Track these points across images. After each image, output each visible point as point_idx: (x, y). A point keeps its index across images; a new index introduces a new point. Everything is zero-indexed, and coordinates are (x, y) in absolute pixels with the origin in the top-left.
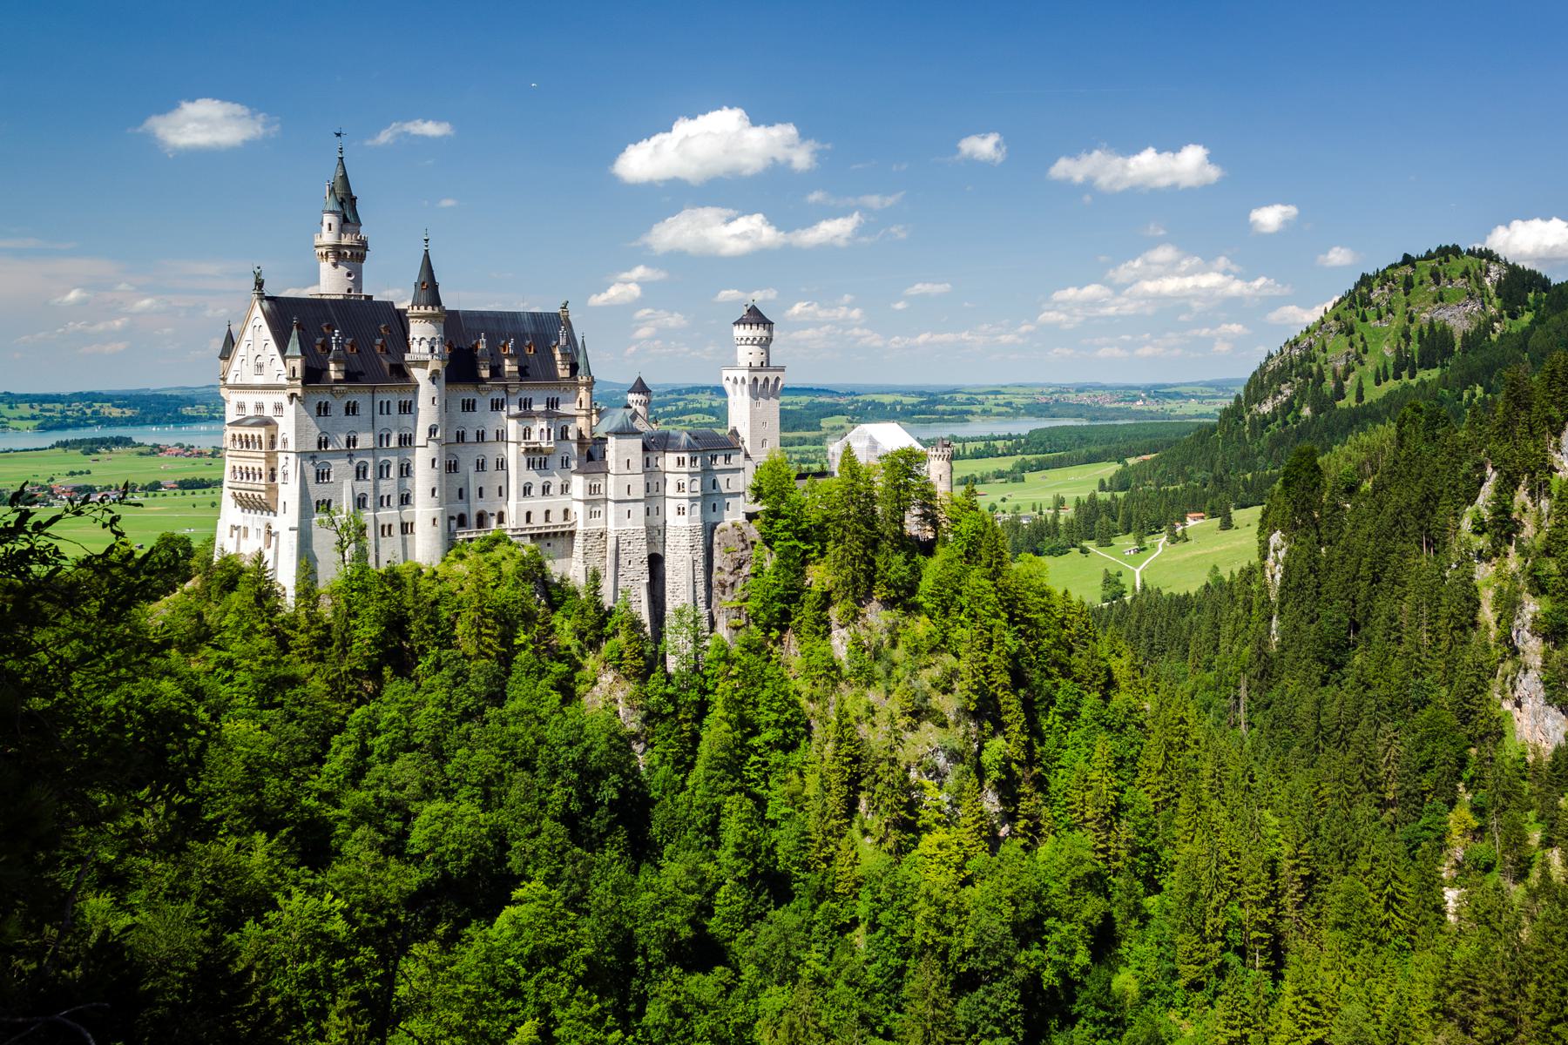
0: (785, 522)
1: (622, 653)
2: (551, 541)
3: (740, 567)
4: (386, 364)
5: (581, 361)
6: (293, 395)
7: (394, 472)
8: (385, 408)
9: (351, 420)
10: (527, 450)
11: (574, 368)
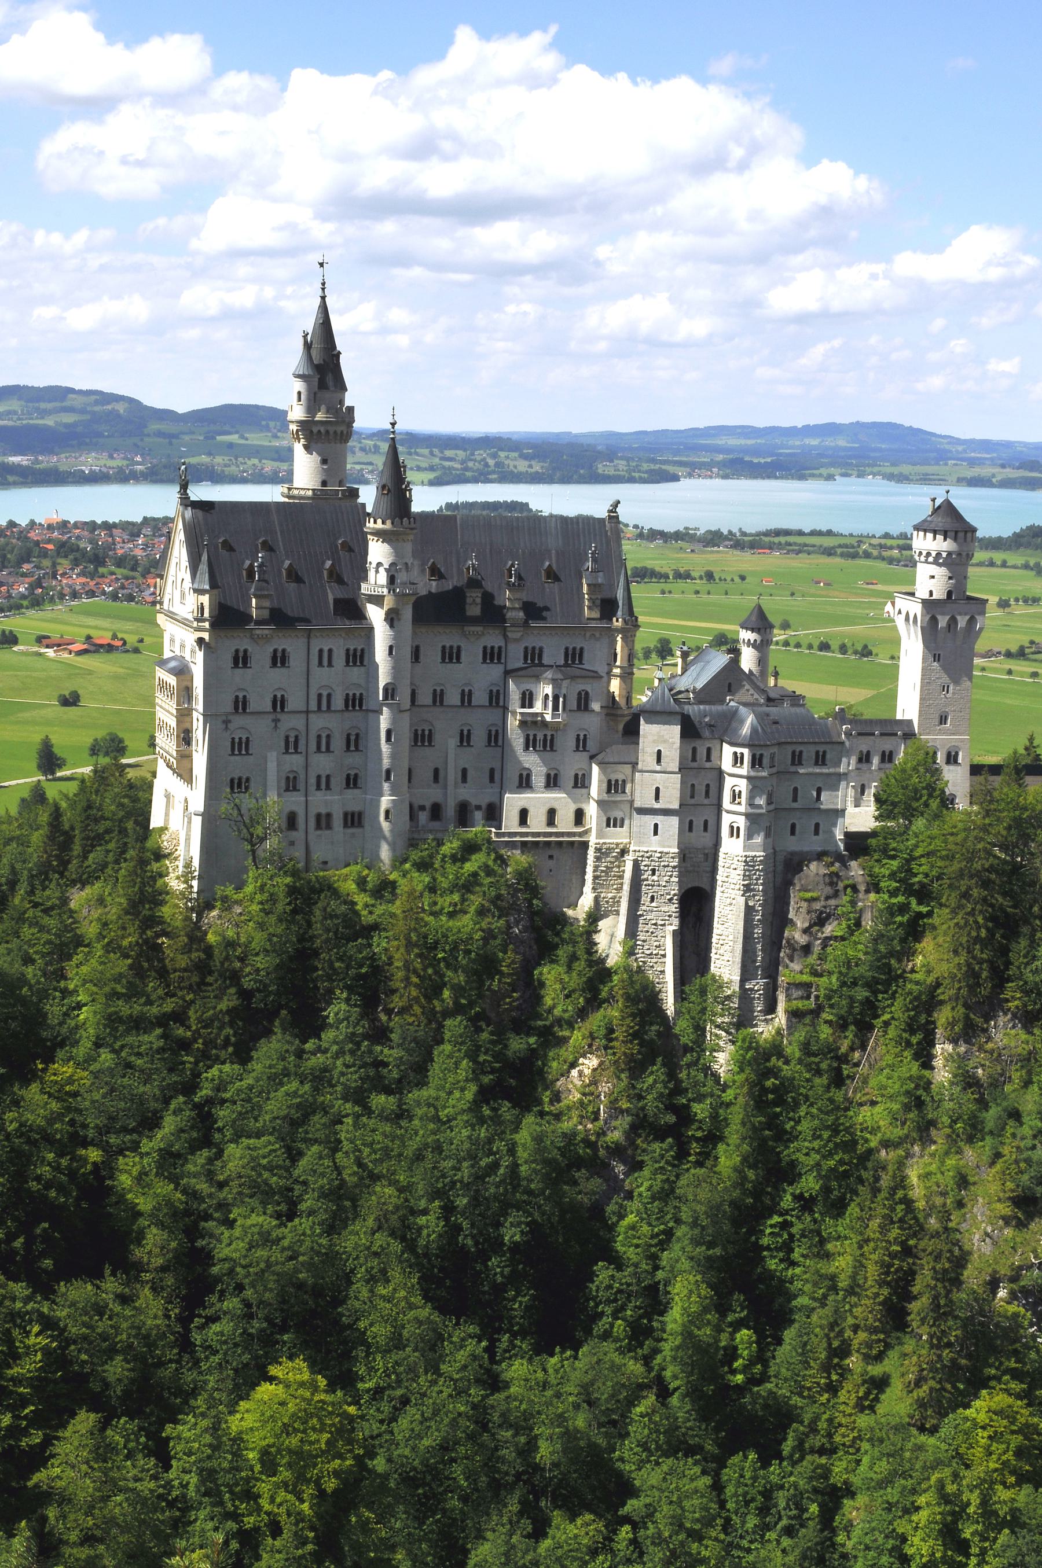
0: (895, 864)
1: (611, 1031)
2: (555, 852)
3: (821, 921)
4: (331, 598)
5: (620, 594)
6: (200, 641)
7: (338, 743)
8: (325, 659)
9: (277, 679)
10: (523, 724)
11: (608, 607)
